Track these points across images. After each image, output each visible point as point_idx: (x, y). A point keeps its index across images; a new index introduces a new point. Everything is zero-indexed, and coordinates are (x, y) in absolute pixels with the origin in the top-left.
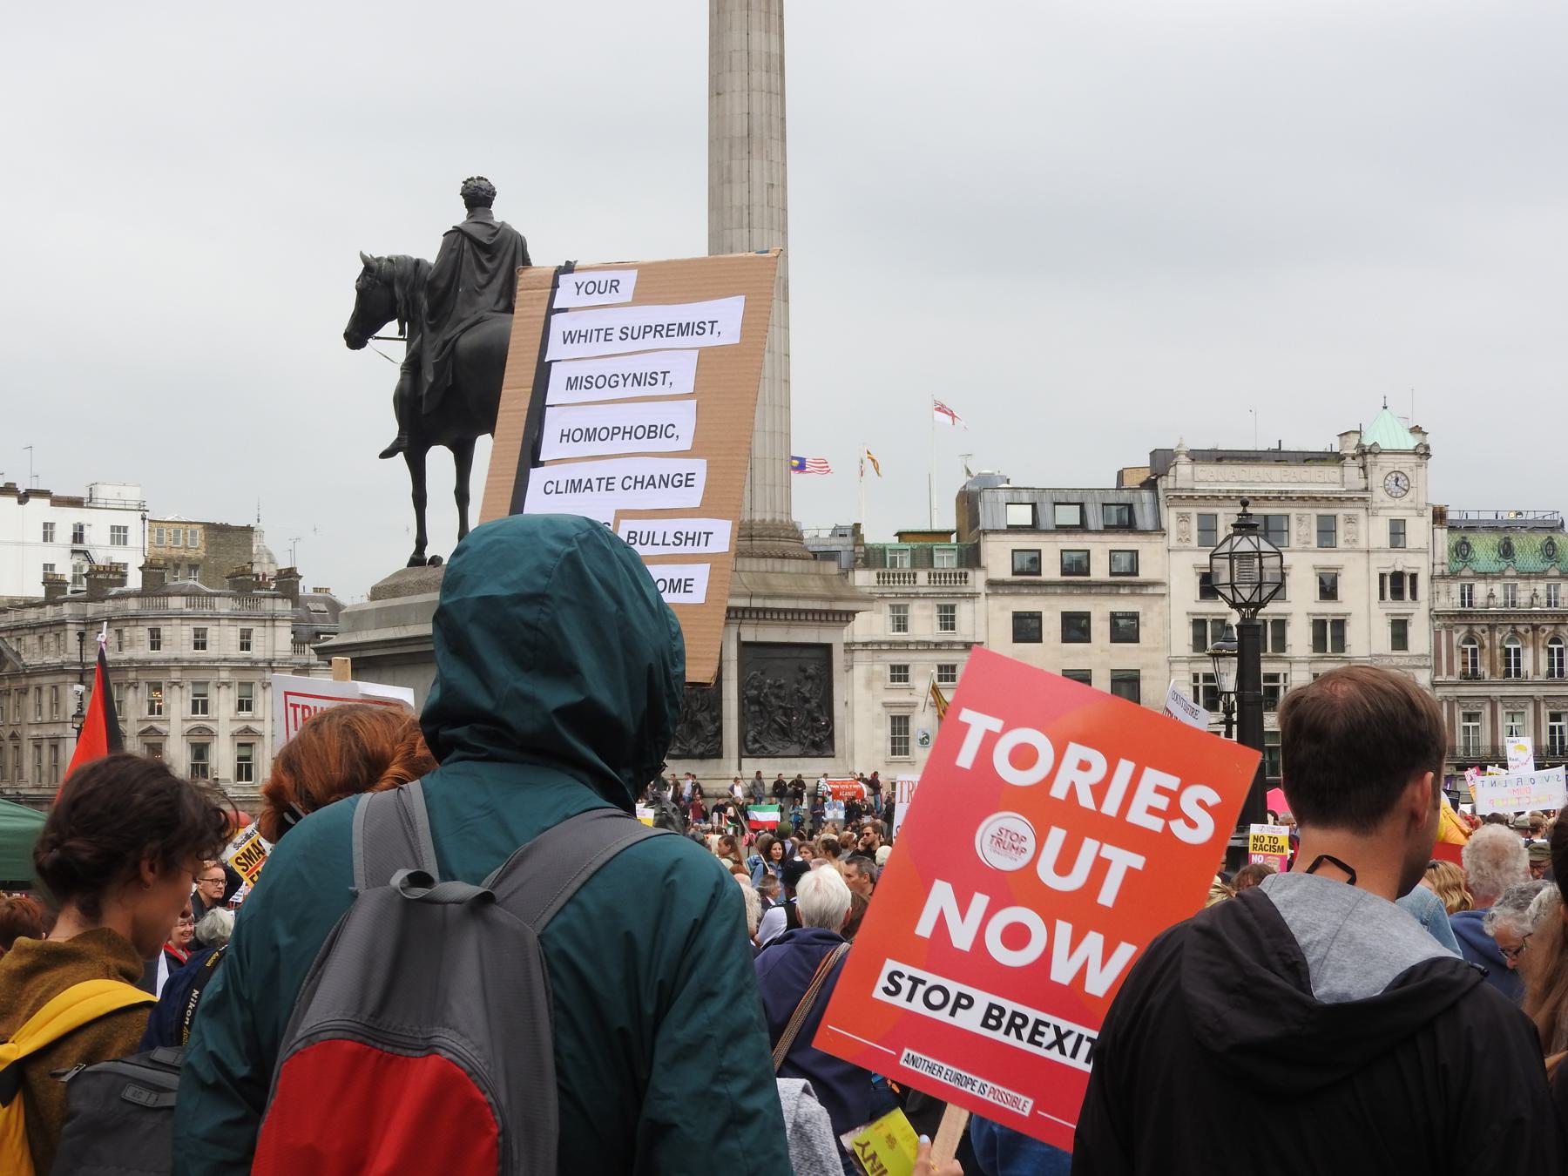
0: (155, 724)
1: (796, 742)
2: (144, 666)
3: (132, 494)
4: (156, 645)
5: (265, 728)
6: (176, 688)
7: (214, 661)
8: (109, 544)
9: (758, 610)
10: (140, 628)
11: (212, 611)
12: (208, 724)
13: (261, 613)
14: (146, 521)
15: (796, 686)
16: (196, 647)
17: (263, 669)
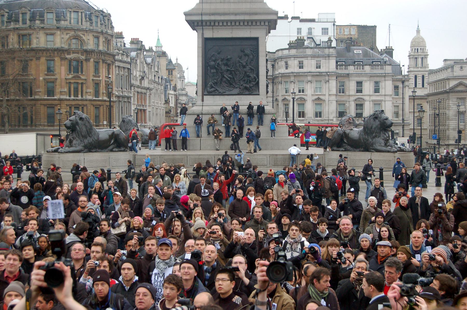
0: (286, 97)
1: (237, 88)
2: (283, 75)
3: (330, 18)
4: (287, 68)
5: (326, 98)
6: (292, 83)
7: (305, 73)
8: (321, 34)
9: (210, 21)
10: (282, 62)
11: (305, 54)
12: (303, 96)
13: (323, 54)
14: (335, 26)
15: (238, 59)
16: (300, 68)
17: (325, 75)
